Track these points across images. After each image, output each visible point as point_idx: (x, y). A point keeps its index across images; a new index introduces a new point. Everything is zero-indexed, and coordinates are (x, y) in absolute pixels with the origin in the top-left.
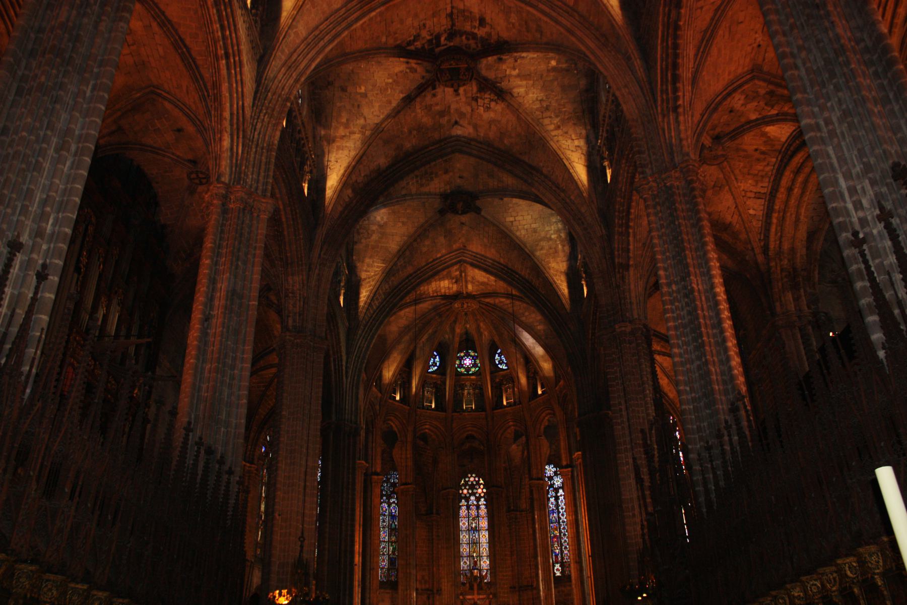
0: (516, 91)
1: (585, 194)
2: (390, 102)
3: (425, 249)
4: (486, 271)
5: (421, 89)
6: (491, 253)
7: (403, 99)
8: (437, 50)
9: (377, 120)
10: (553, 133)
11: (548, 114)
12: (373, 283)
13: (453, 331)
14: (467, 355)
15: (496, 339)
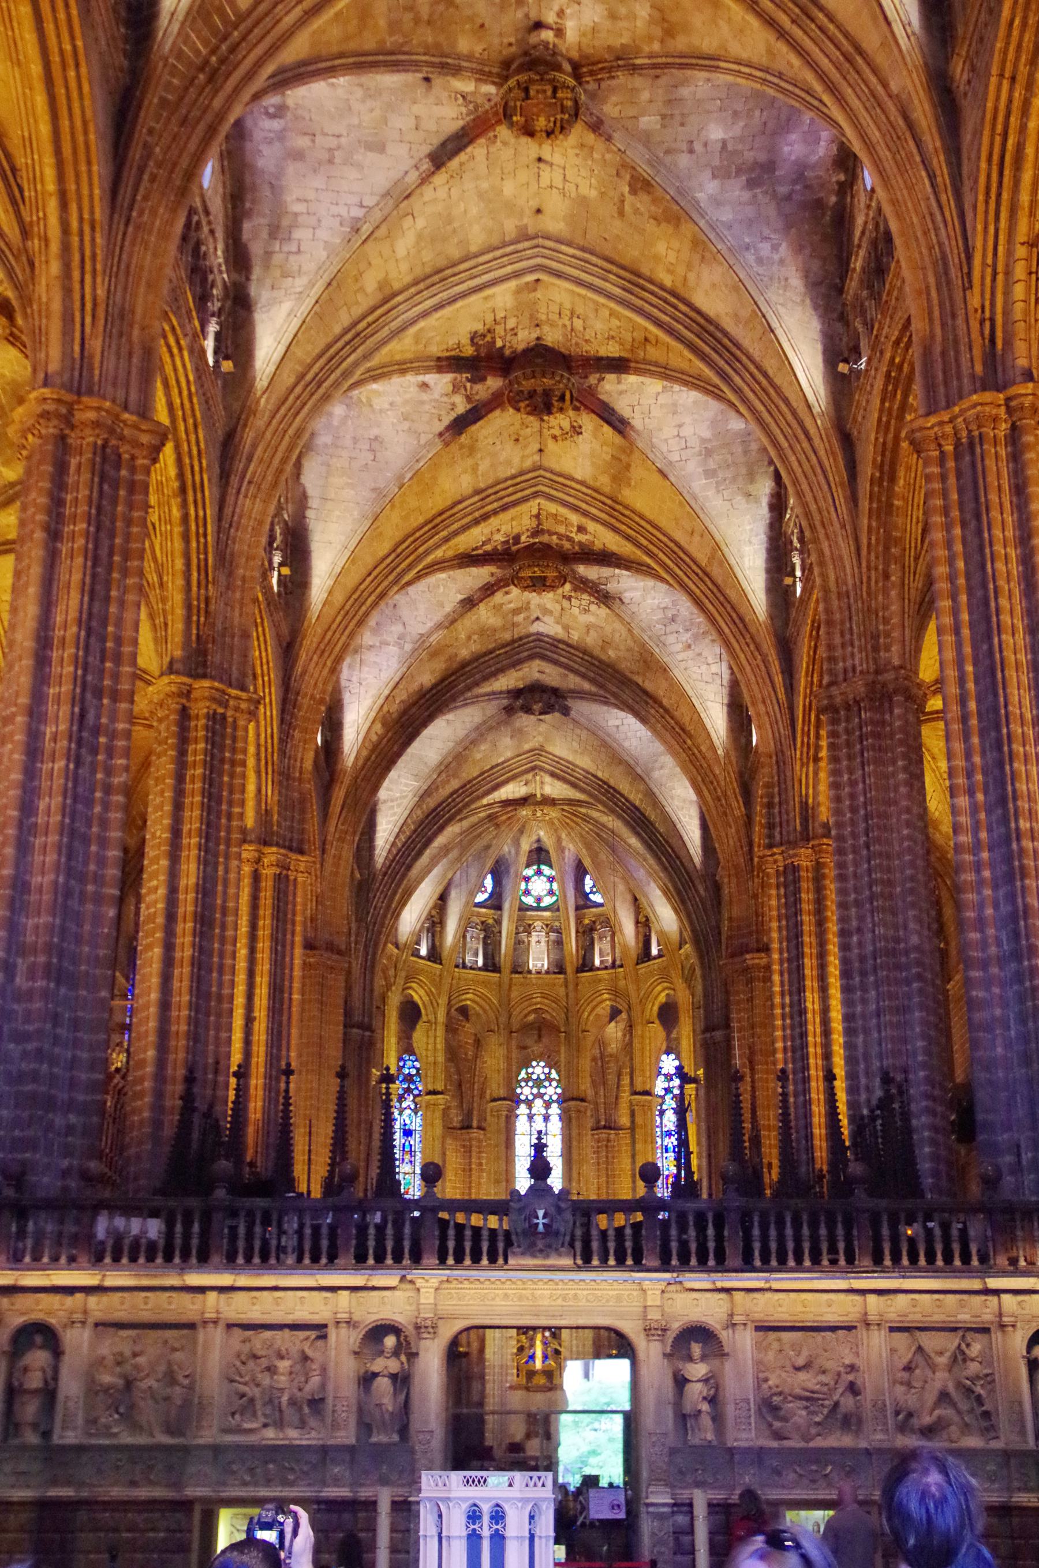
0: (627, 596)
1: (720, 752)
2: (441, 605)
3: (478, 756)
4: (574, 786)
5: (489, 590)
6: (585, 762)
7: (462, 601)
8: (514, 548)
9: (423, 630)
10: (680, 657)
11: (674, 627)
12: (398, 810)
13: (517, 843)
14: (539, 873)
15: (587, 863)
